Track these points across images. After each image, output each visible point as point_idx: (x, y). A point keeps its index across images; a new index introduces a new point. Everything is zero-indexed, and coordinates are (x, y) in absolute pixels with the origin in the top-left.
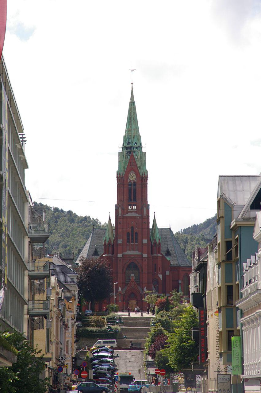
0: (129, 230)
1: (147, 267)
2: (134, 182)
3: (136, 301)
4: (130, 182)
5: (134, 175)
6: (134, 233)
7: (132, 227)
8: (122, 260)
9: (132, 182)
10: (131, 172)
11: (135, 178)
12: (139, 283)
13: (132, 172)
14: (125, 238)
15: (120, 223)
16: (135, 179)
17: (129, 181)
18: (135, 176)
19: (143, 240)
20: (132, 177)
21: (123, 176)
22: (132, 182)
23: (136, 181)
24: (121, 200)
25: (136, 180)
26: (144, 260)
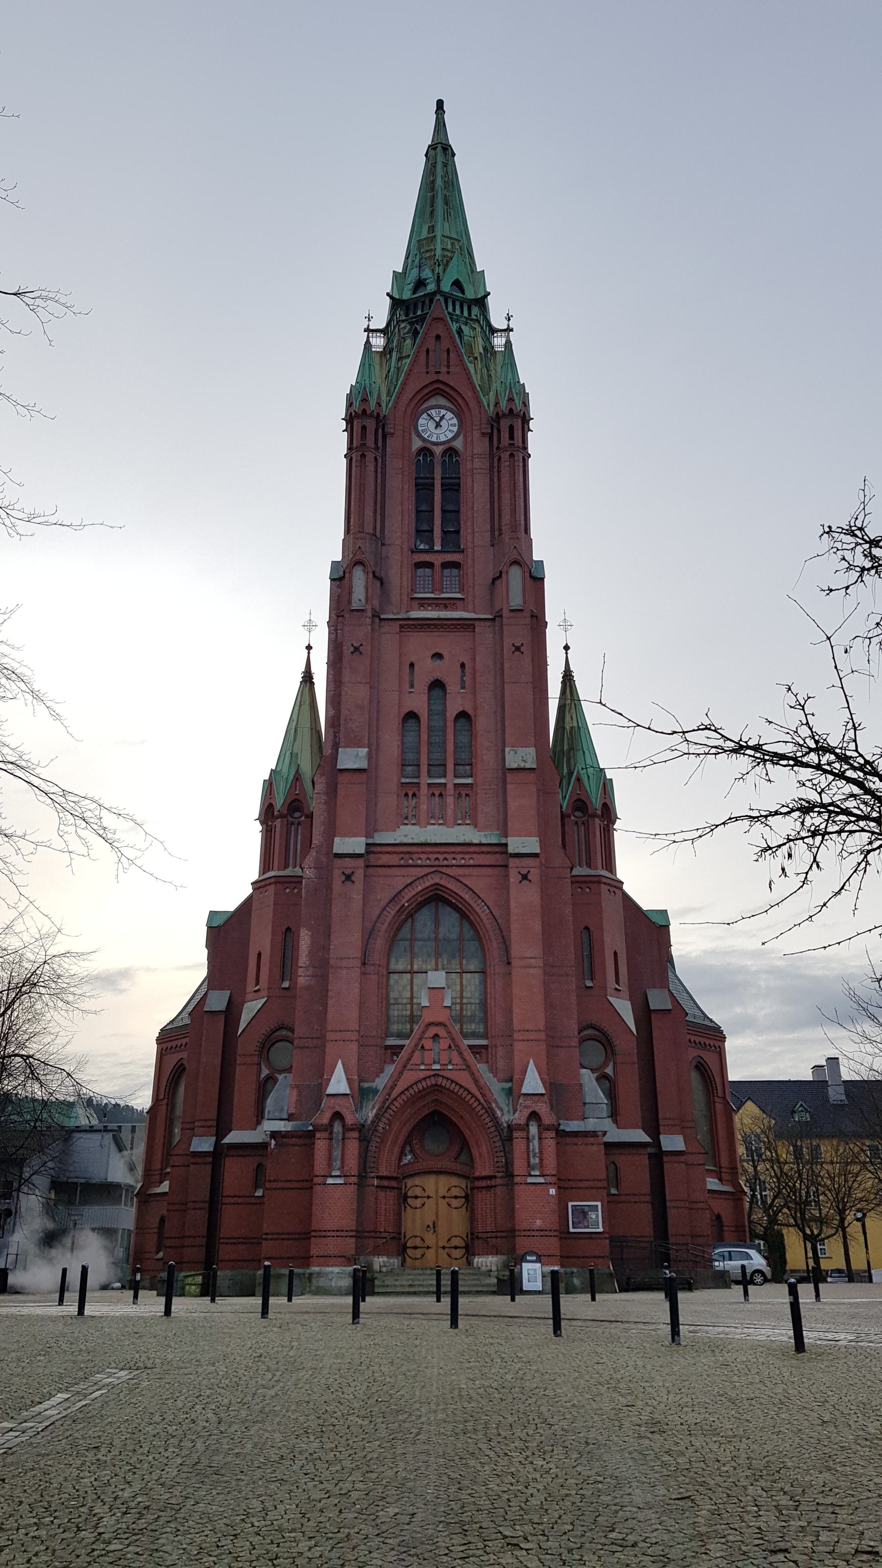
0: (418, 702)
1: (537, 926)
2: (450, 452)
3: (463, 1183)
4: (425, 451)
6: (451, 714)
7: (437, 685)
8: (359, 876)
9: (438, 450)
10: (432, 402)
11: (455, 429)
13: (442, 401)
14: (391, 741)
15: (356, 649)
16: (454, 438)
17: (417, 444)
18: (455, 421)
20: (439, 427)
21: (384, 411)
22: (438, 450)
23: (458, 444)
24: (369, 529)
25: (461, 439)
26: (514, 878)
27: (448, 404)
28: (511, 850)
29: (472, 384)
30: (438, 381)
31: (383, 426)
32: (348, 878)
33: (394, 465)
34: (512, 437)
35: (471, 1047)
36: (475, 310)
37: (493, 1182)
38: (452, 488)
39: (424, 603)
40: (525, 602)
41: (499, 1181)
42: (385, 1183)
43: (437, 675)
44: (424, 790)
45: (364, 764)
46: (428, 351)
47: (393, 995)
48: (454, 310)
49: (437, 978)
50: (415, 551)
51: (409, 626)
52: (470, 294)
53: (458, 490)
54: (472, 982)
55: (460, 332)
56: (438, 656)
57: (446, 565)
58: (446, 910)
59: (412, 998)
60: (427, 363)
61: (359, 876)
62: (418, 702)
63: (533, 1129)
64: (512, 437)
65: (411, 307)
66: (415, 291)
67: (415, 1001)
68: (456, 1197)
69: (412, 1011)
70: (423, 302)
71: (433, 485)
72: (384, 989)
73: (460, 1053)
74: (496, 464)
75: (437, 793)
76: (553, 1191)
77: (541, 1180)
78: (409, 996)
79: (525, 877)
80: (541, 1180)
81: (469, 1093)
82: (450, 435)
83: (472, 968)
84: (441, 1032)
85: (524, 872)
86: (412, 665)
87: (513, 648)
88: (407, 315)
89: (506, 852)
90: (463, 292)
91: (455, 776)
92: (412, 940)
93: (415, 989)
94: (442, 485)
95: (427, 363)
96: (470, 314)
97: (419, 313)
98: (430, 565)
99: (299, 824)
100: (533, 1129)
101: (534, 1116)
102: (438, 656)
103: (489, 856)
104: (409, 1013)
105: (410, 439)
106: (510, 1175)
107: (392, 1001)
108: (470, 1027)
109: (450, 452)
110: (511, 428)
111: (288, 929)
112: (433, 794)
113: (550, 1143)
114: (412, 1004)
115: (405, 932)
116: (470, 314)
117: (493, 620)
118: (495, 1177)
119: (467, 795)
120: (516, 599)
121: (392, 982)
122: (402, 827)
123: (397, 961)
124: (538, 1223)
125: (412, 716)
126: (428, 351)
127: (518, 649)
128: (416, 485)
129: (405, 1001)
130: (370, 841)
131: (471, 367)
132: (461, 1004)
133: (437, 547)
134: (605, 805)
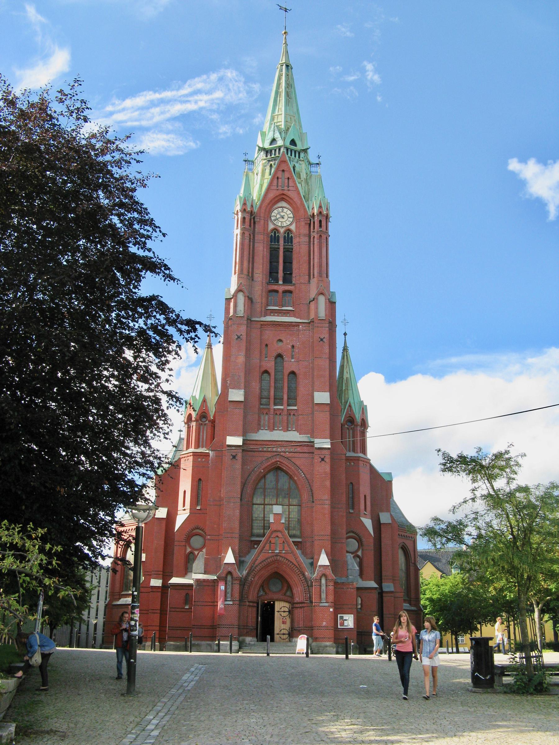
0: (270, 365)
1: (328, 483)
3: (287, 605)
4: (275, 230)
5: (289, 212)
6: (286, 372)
9: (282, 230)
10: (280, 204)
11: (291, 220)
12: (299, 540)
13: (283, 204)
14: (255, 386)
15: (239, 337)
16: (291, 224)
17: (271, 227)
18: (291, 215)
19: (316, 394)
20: (283, 218)
21: (255, 210)
22: (282, 230)
23: (293, 227)
25: (294, 225)
26: (317, 459)
27: (288, 206)
28: (316, 446)
29: (299, 193)
30: (283, 194)
31: (254, 218)
32: (234, 457)
33: (259, 237)
34: (321, 226)
35: (293, 542)
36: (302, 155)
37: (303, 605)
38: (288, 252)
39: (273, 312)
40: (326, 315)
41: (305, 605)
42: (251, 604)
43: (280, 351)
44: (272, 411)
45: (241, 398)
46: (278, 178)
47: (255, 515)
48: (291, 155)
49: (278, 509)
50: (269, 283)
51: (265, 325)
52: (299, 147)
53: (292, 252)
54: (294, 509)
55: (294, 167)
56: (280, 340)
57: (285, 292)
58: (281, 474)
59: (264, 517)
60: (277, 184)
61: (240, 455)
62: (270, 365)
63: (323, 581)
64: (321, 226)
65: (269, 152)
66: (271, 144)
67: (266, 519)
68: (284, 612)
69: (264, 524)
70: (275, 150)
71: (279, 248)
72: (250, 513)
73: (289, 545)
74: (312, 240)
75: (278, 413)
76: (331, 610)
77: (327, 604)
78: (262, 516)
79: (323, 459)
80: (327, 604)
81: (293, 564)
82: (289, 223)
83: (295, 503)
84: (280, 535)
85: (322, 457)
86: (267, 345)
87: (320, 340)
88: (267, 156)
89: (313, 446)
90: (296, 145)
91: (288, 405)
92: (265, 489)
93: (266, 513)
94: (284, 248)
95: (277, 184)
96: (299, 157)
97: (273, 156)
98: (277, 291)
99: (205, 424)
100: (323, 581)
101: (324, 575)
102: (280, 340)
103: (305, 448)
104: (262, 525)
105: (268, 225)
106: (311, 602)
107: (254, 518)
108: (293, 532)
109: (289, 231)
110: (320, 221)
111: (200, 480)
112: (276, 414)
113: (331, 588)
114: (264, 520)
115: (261, 484)
116: (299, 157)
117: (309, 323)
118: (304, 603)
119: (294, 415)
120: (322, 314)
121: (254, 509)
122: (260, 431)
123: (257, 498)
124: (324, 623)
125: (266, 372)
126: (278, 178)
127: (322, 340)
128: (270, 248)
129: (260, 519)
130: (245, 438)
131: (299, 186)
132: (289, 521)
133: (281, 282)
134: (363, 420)
